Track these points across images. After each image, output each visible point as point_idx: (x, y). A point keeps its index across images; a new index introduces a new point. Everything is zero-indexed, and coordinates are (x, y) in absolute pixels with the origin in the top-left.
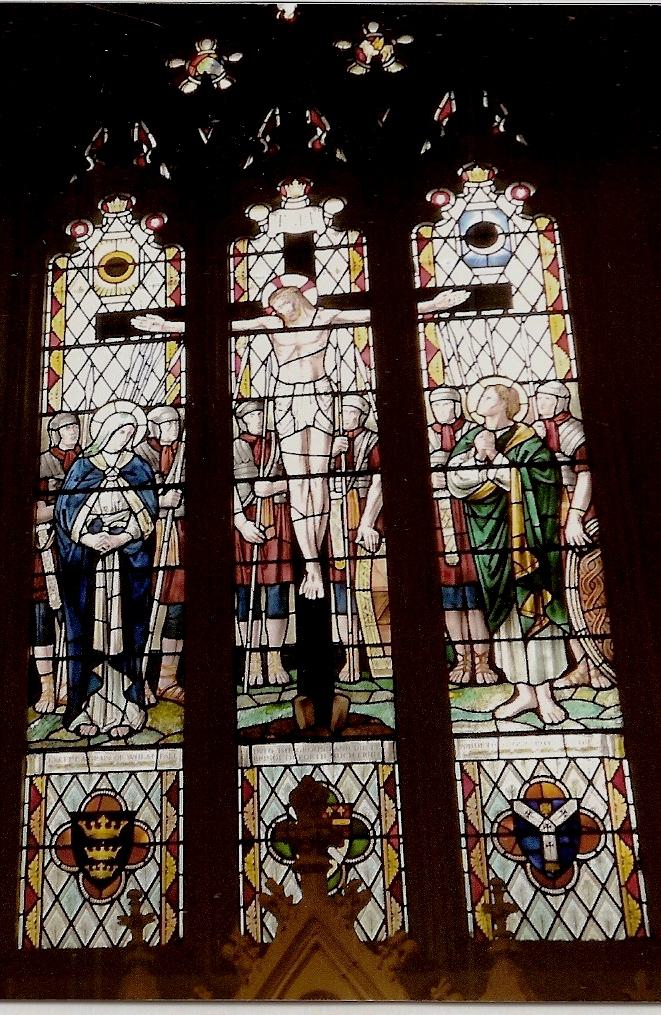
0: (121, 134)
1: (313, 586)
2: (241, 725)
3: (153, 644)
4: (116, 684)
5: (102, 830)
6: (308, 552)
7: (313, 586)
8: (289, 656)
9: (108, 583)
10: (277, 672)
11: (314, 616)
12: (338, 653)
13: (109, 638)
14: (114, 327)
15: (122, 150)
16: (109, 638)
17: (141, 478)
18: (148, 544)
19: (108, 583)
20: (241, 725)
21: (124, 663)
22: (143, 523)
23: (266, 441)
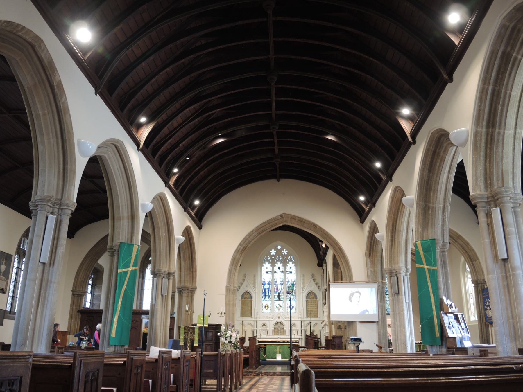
0: (267, 257)
1: (279, 292)
2: (180, 344)
3: (269, 295)
4: (267, 297)
5: (267, 306)
6: (279, 289)
7: (279, 292)
8: (277, 296)
9: (267, 291)
10: (277, 297)
11: (279, 293)
12: (280, 296)
13: (267, 294)
14: (267, 273)
15: (267, 259)
16: (267, 294)
17: (269, 284)
18: (269, 288)
19: (267, 291)
20: (180, 344)
21: (268, 296)
22: (269, 287)
23: (276, 282)
